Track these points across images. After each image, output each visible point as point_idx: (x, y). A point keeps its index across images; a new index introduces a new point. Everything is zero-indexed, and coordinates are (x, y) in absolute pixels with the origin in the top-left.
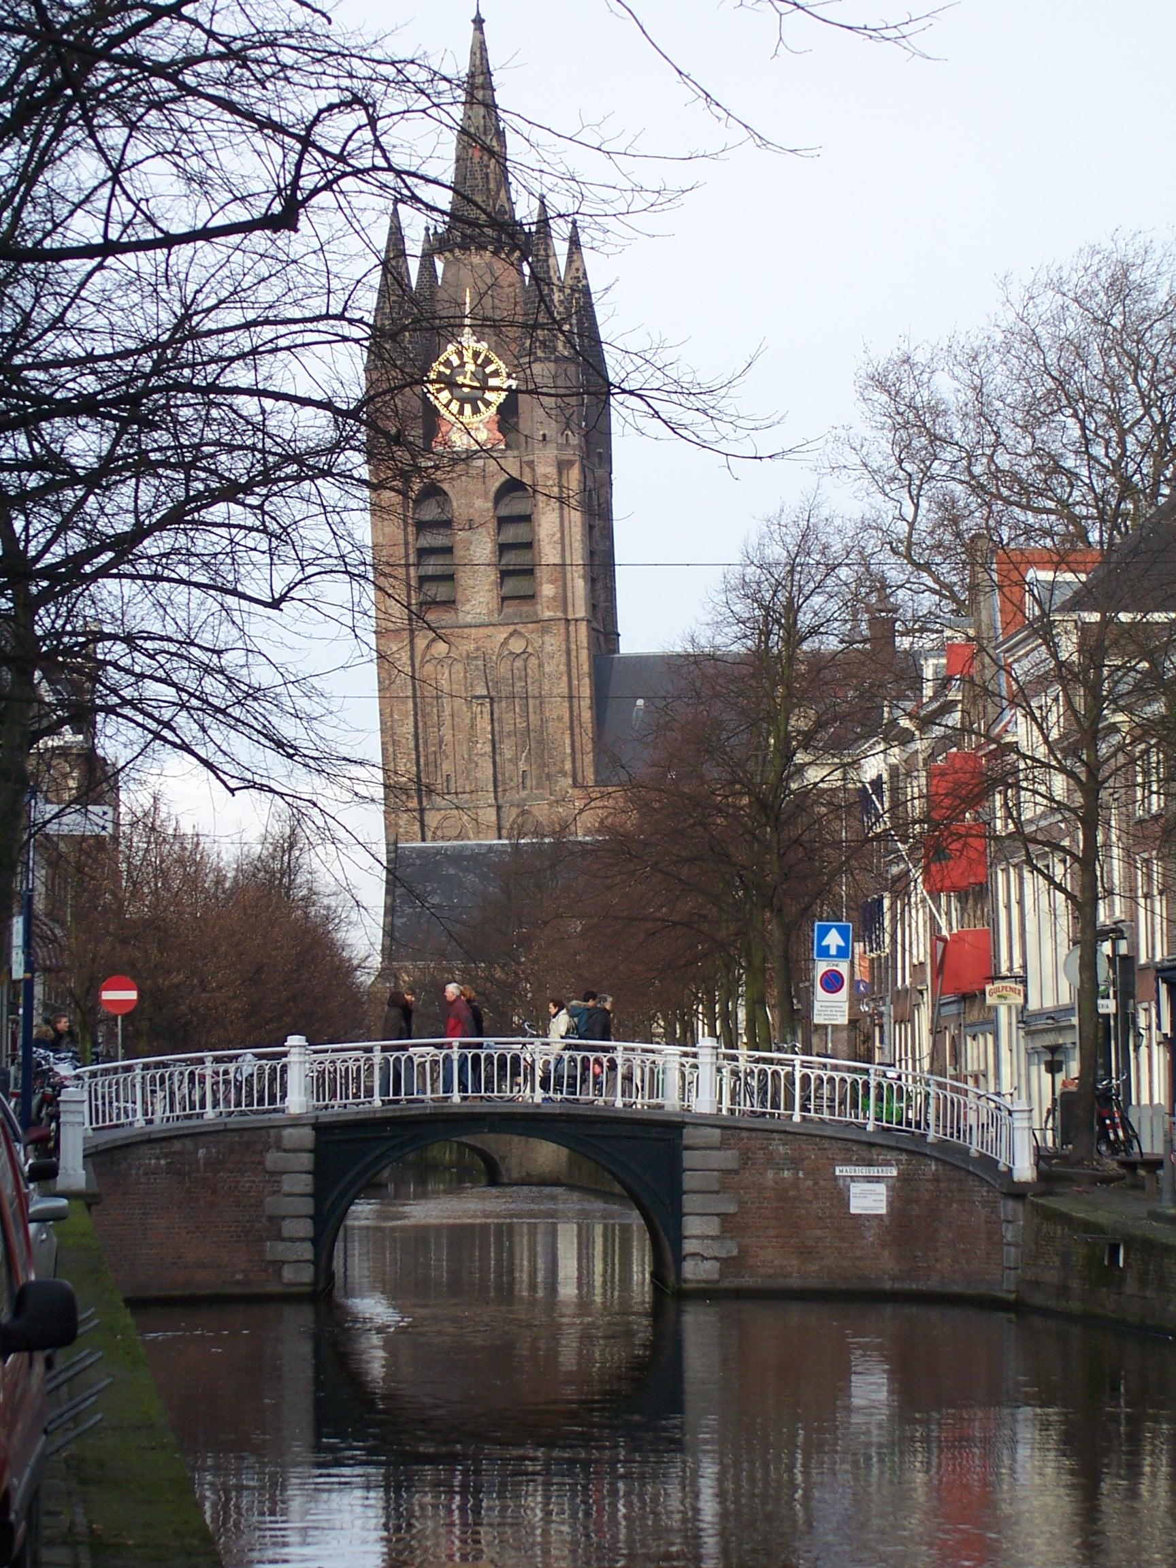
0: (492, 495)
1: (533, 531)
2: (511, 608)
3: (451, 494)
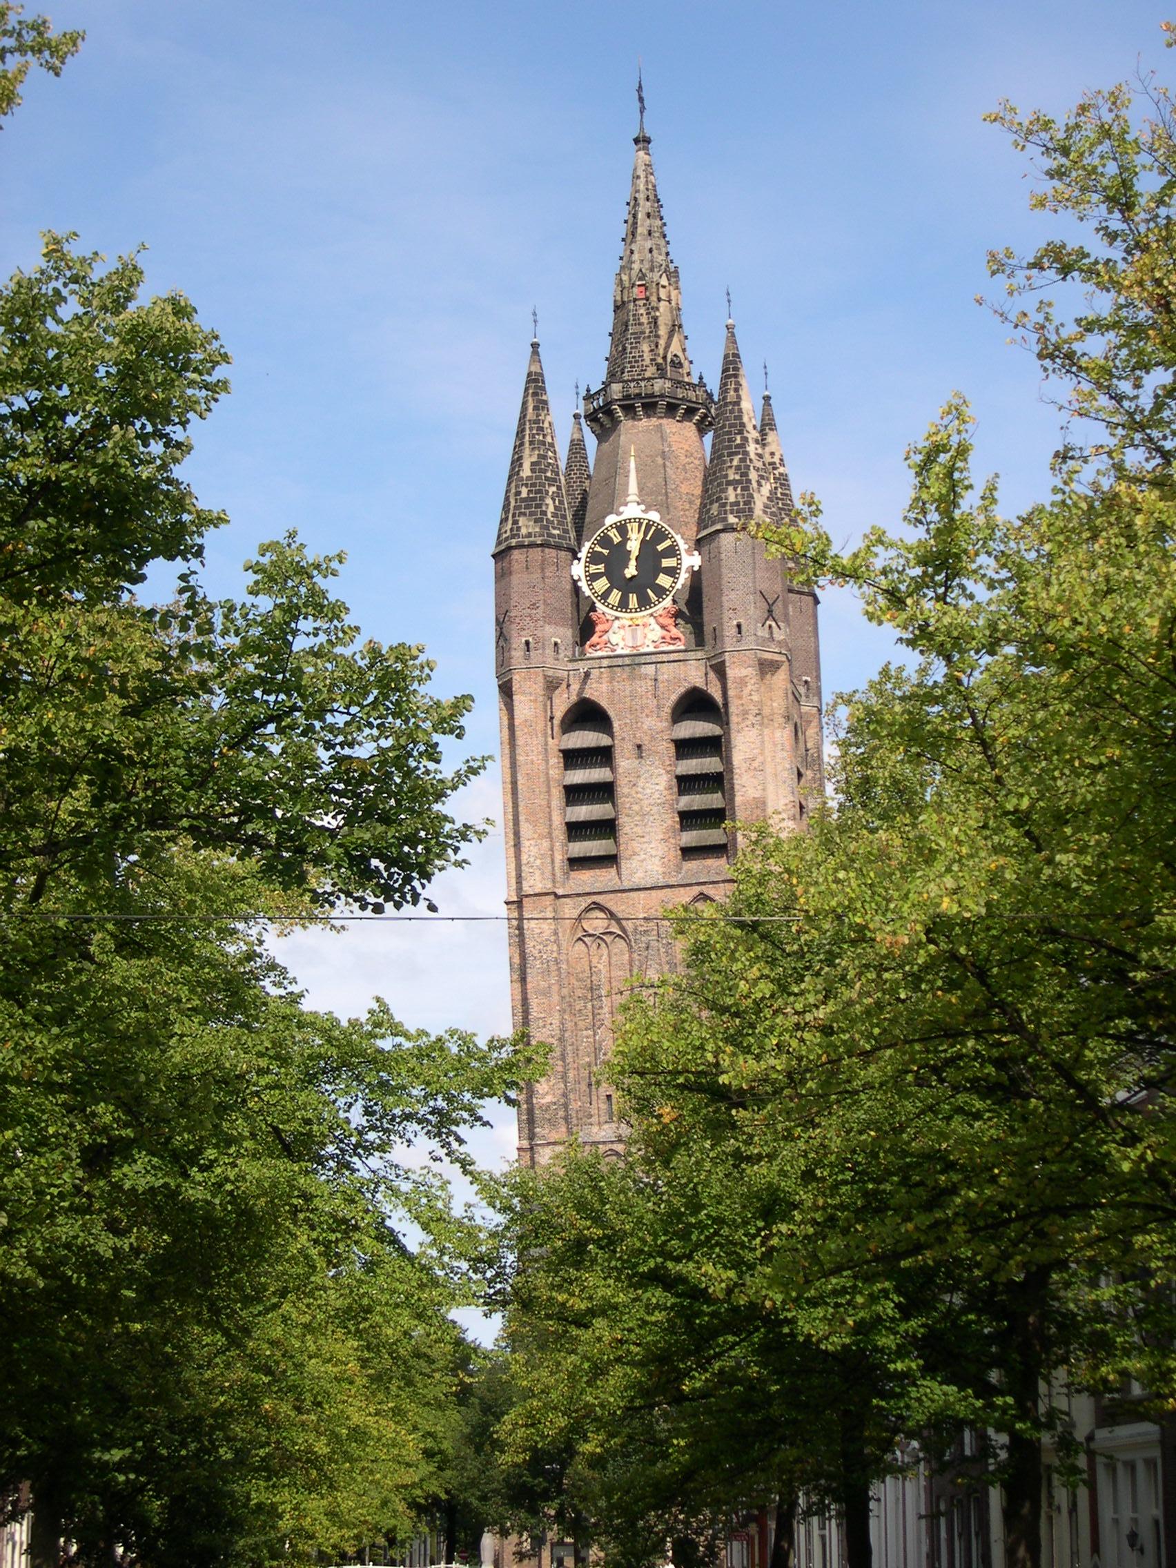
0: (667, 710)
1: (727, 761)
3: (611, 713)
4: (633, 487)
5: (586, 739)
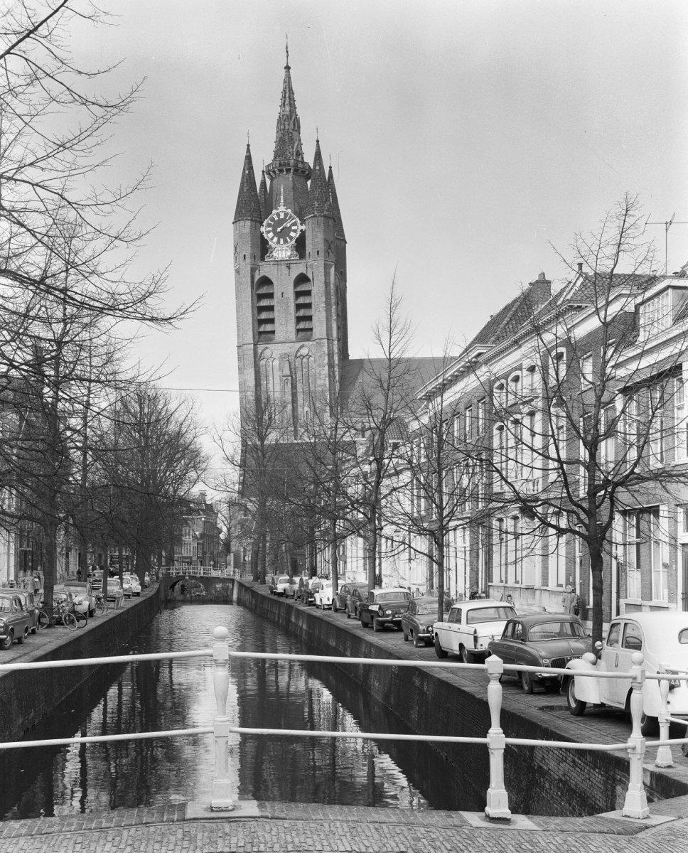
2: (301, 334)
4: (282, 200)
5: (264, 290)
